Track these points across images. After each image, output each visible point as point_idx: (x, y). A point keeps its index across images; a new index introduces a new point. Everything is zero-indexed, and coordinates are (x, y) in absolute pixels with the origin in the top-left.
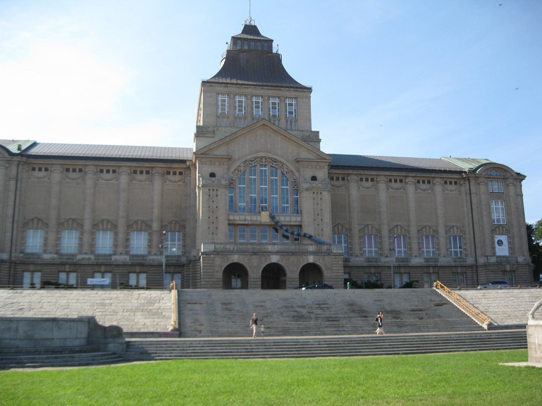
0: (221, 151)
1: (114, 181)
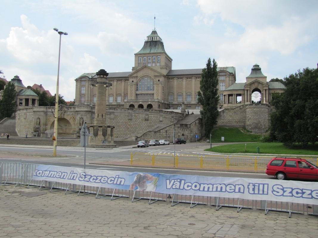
0: (135, 75)
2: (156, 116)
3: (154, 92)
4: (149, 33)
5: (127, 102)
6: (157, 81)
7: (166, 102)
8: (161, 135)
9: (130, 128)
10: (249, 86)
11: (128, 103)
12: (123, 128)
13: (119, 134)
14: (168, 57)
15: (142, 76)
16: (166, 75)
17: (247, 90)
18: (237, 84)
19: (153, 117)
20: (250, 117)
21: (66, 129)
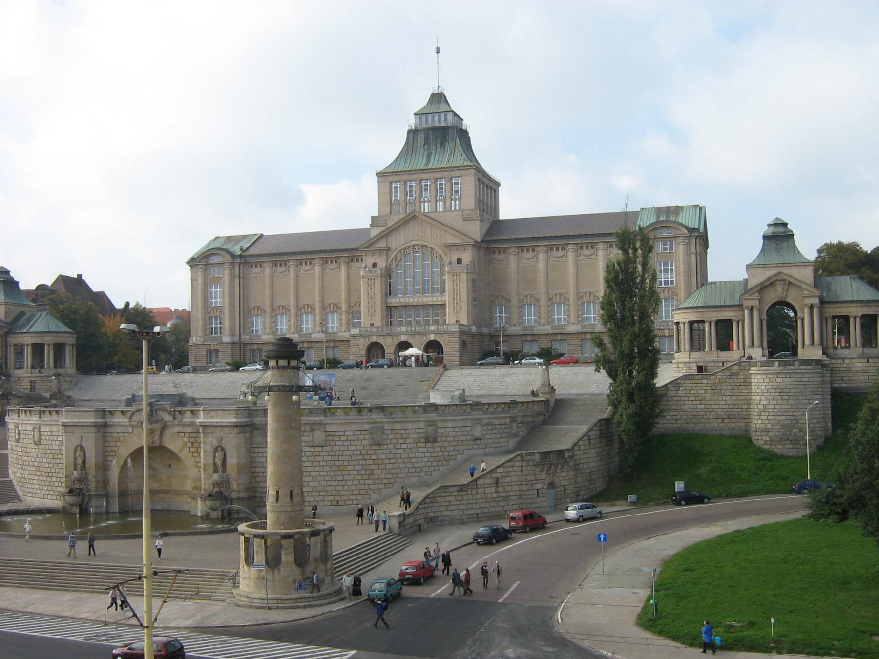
0: (382, 244)
1: (311, 271)
2: (460, 424)
3: (443, 298)
4: (421, 102)
5: (361, 336)
6: (454, 260)
7: (485, 330)
8: (479, 497)
9: (379, 472)
10: (757, 294)
11: (361, 341)
12: (355, 473)
13: (345, 493)
14: (487, 182)
15: (403, 247)
16: (482, 241)
17: (751, 310)
18: (718, 284)
19: (452, 429)
20: (765, 402)
21: (169, 477)
